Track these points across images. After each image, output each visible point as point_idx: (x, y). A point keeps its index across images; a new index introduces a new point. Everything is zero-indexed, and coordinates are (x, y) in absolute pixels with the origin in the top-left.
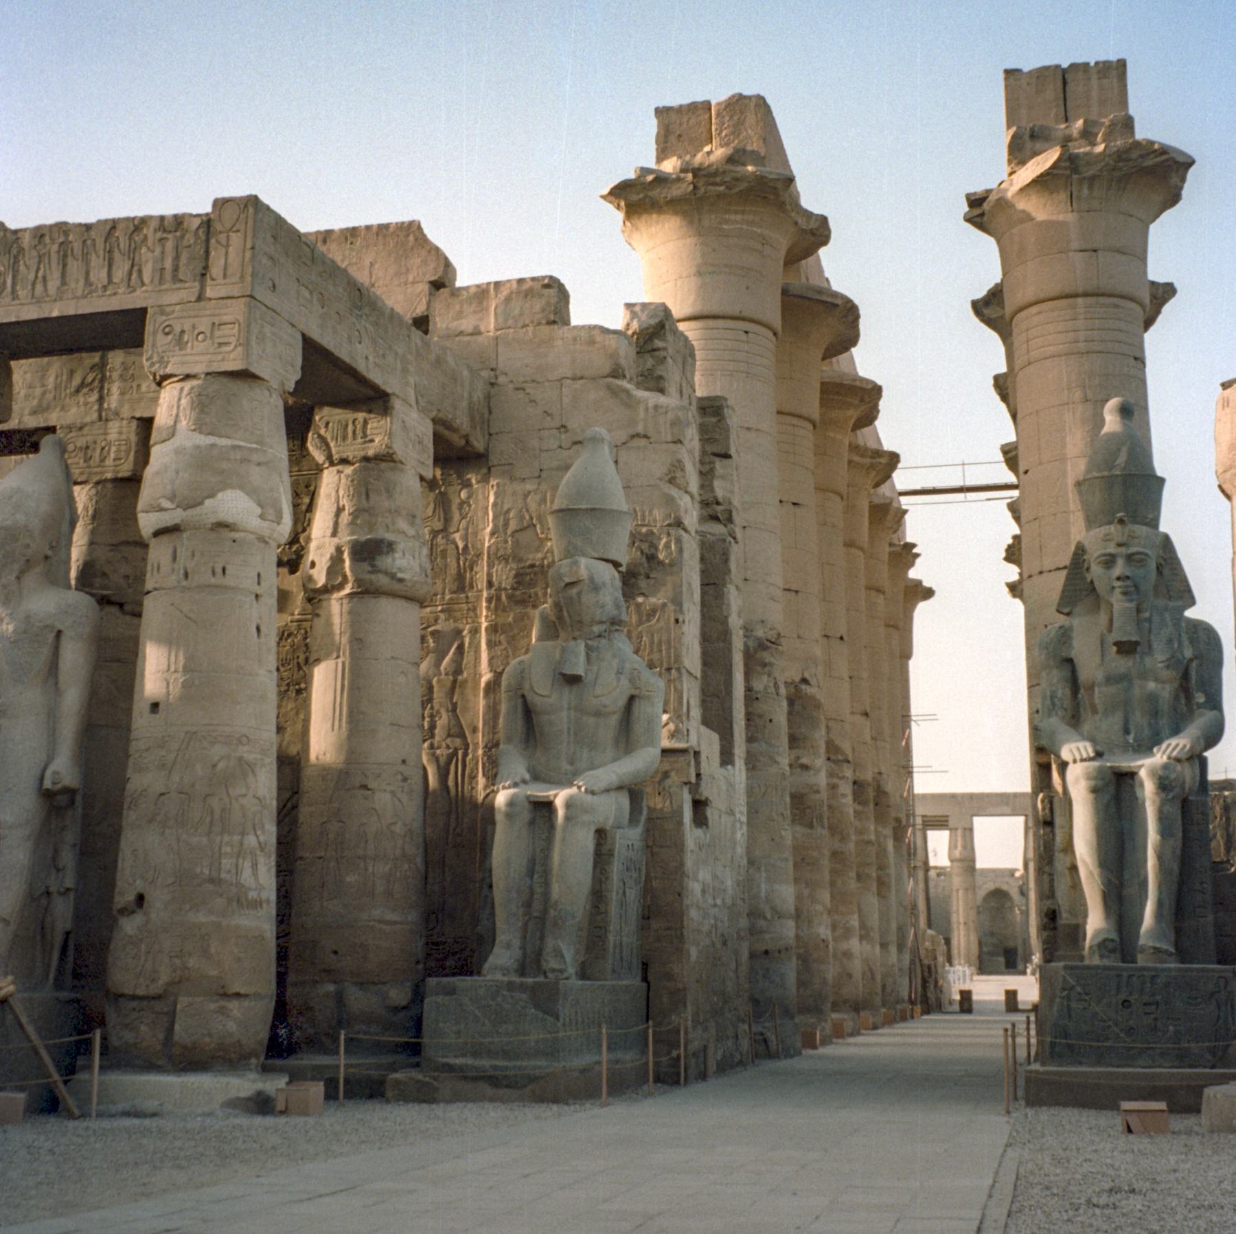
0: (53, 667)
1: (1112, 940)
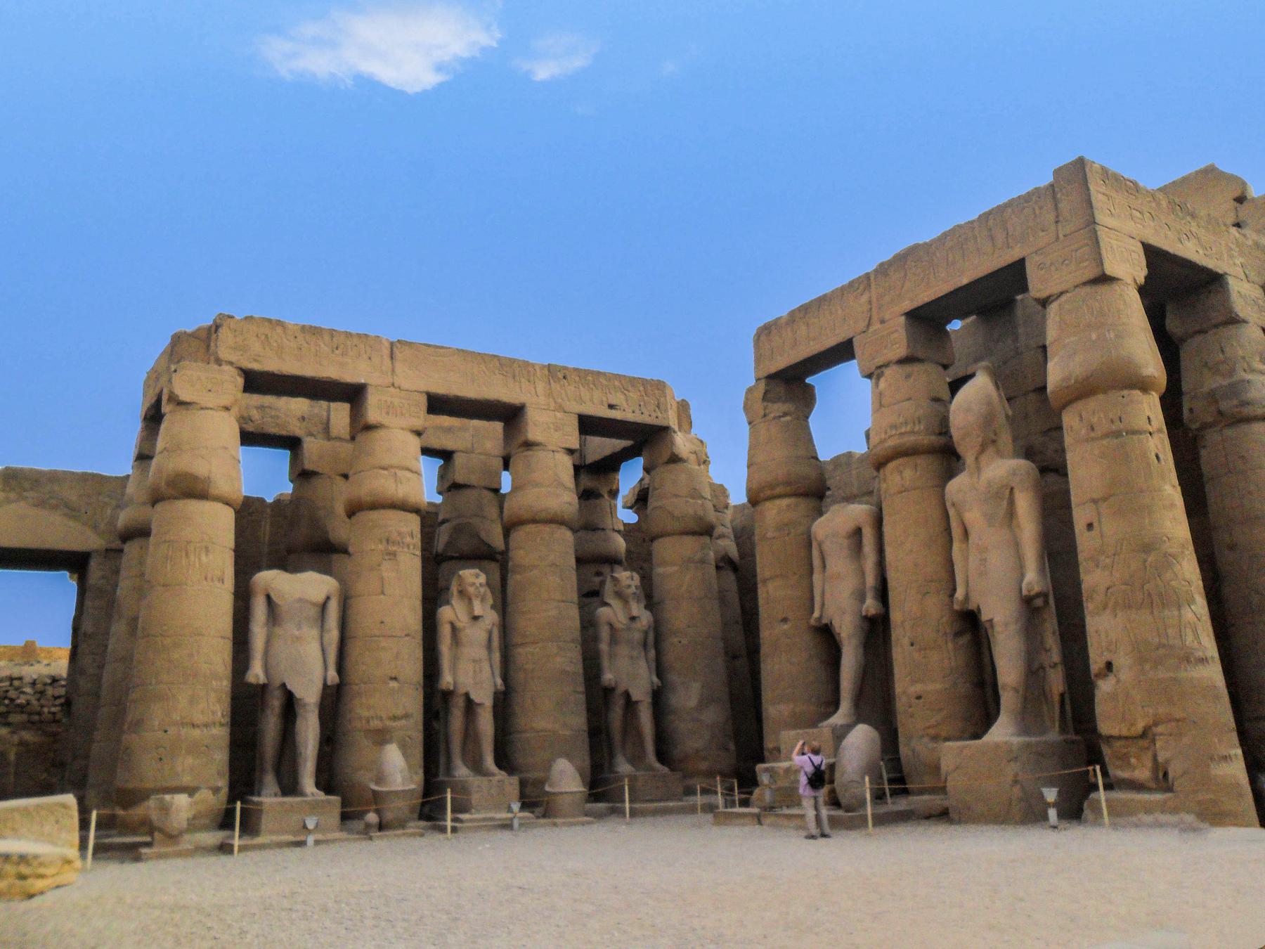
0: (1011, 513)
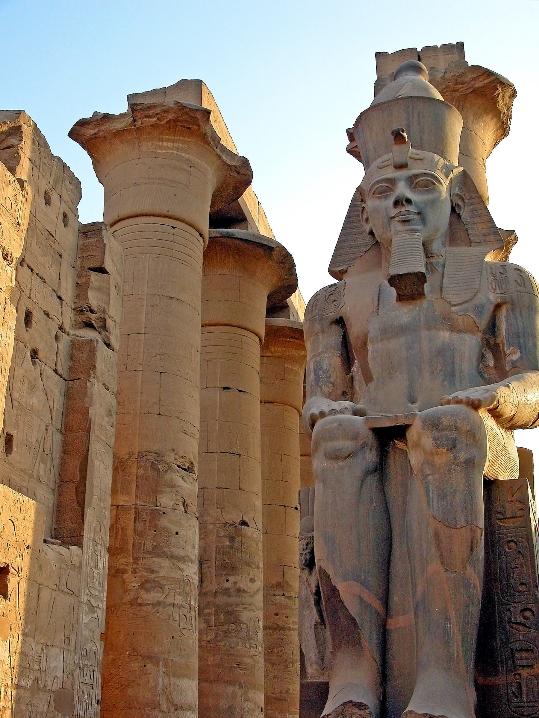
1: (359, 706)
